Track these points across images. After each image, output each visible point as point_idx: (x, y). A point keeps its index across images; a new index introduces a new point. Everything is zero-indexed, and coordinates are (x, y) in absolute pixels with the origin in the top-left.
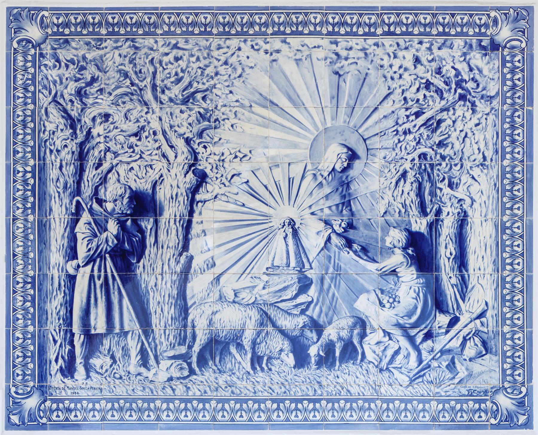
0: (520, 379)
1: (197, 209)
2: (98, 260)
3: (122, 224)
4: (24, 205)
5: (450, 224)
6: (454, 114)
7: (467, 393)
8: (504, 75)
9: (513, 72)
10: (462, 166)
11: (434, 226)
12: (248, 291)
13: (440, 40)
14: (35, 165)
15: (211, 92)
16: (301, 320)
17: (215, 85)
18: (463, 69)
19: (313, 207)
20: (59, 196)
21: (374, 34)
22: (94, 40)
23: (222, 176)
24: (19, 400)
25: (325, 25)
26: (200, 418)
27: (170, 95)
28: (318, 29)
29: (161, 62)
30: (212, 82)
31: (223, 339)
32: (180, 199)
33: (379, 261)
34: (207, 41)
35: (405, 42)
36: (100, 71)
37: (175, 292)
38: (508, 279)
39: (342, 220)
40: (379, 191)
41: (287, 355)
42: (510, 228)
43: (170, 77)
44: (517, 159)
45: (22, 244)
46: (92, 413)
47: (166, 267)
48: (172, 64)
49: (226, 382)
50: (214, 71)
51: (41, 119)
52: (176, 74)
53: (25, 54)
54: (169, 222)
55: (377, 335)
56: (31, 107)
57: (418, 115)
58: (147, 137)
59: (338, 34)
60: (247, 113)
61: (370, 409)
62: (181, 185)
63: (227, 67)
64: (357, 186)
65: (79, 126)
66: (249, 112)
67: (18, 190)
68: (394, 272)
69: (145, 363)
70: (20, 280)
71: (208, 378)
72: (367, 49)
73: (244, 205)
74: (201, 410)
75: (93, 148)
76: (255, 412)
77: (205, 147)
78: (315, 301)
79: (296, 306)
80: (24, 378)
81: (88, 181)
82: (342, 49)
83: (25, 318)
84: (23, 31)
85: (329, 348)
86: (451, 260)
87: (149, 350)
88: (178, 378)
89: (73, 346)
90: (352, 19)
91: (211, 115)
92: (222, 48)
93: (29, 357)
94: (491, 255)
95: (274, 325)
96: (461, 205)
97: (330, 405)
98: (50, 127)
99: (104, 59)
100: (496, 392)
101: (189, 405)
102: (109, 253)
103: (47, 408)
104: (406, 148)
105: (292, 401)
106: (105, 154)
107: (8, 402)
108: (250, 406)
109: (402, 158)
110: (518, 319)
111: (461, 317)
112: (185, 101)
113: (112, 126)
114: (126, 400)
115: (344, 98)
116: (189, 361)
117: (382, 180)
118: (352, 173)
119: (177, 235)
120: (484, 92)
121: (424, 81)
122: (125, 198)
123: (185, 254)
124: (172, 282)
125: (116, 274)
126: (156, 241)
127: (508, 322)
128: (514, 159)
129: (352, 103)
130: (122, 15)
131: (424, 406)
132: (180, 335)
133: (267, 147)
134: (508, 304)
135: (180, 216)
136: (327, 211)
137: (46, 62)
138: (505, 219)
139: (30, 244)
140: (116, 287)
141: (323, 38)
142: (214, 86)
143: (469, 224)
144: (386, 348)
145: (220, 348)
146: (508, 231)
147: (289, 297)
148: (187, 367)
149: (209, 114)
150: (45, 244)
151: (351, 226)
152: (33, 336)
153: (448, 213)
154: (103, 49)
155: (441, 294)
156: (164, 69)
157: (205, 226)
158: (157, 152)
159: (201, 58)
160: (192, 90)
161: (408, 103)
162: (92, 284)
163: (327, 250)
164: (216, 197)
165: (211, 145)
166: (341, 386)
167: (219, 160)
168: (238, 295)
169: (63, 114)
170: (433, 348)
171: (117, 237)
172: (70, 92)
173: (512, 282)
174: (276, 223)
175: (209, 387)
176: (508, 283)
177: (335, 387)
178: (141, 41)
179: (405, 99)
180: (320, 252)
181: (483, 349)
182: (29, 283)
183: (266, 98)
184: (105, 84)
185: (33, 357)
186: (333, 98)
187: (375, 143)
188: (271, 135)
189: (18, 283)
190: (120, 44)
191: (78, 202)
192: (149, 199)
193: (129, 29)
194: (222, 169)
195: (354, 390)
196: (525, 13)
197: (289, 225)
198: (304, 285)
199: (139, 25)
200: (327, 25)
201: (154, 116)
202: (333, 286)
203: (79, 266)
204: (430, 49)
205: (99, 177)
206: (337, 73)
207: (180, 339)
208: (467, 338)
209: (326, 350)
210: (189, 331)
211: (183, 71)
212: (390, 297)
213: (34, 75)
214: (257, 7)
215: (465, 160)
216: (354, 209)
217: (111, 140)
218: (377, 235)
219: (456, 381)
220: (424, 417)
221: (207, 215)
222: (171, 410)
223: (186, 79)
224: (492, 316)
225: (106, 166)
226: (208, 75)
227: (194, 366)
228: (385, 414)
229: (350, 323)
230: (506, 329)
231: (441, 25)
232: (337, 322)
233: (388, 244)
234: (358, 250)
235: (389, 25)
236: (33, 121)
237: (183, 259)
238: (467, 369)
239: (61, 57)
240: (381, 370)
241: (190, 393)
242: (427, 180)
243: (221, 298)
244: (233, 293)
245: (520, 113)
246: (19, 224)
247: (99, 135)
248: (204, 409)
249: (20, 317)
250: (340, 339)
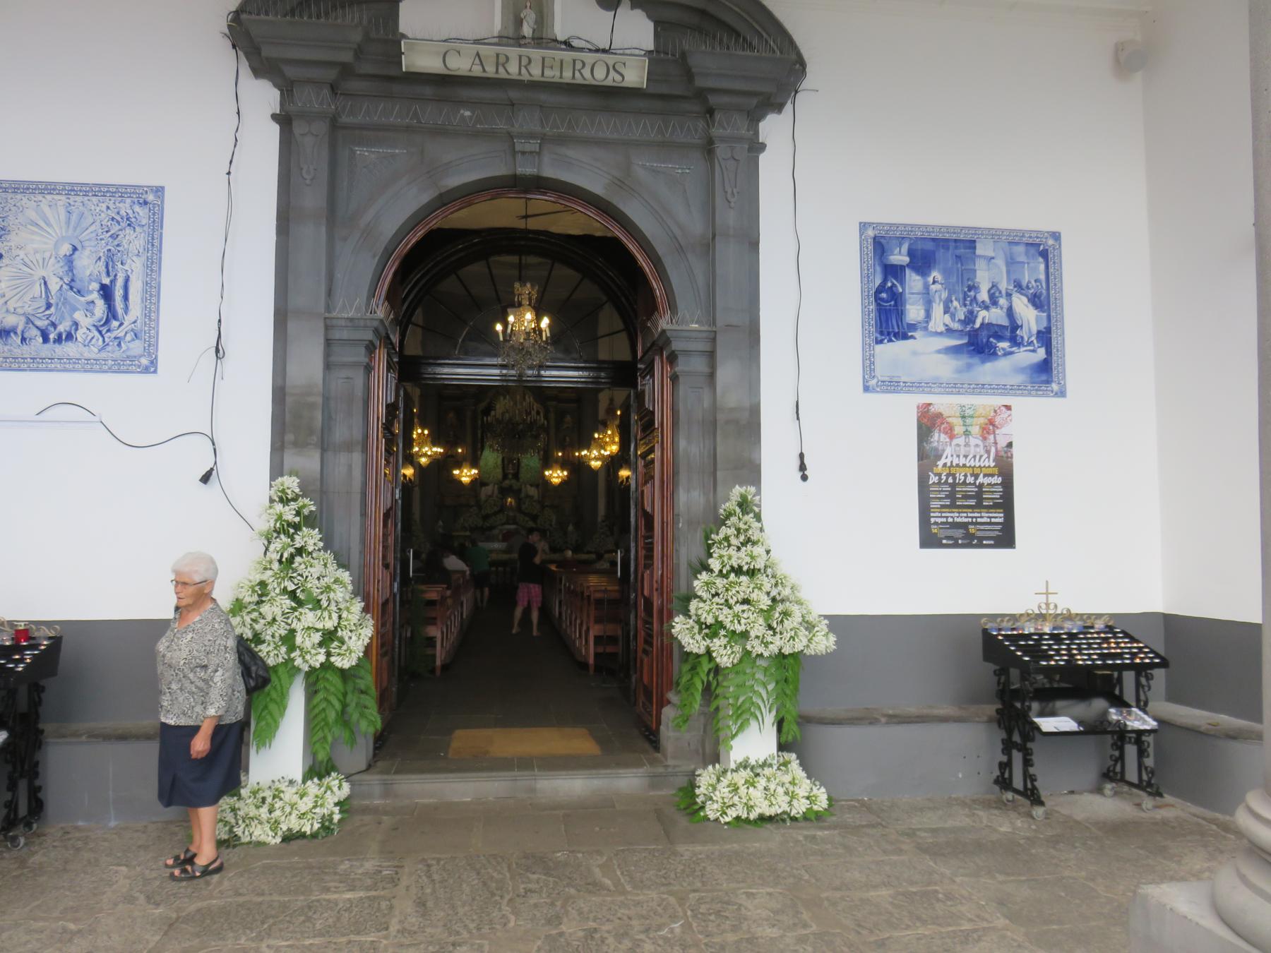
16: (46, 322)
40: (88, 265)
85: (60, 335)
100: (141, 356)
151: (73, 280)
174: (36, 278)
198: (49, 306)
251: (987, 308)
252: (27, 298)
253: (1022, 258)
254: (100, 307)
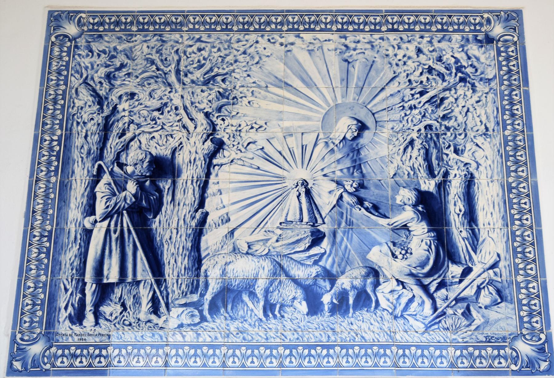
0: (538, 326)
1: (214, 172)
2: (116, 216)
3: (140, 185)
4: (47, 168)
5: (458, 185)
6: (456, 93)
7: (484, 339)
8: (500, 63)
9: (508, 59)
10: (466, 135)
11: (442, 186)
12: (261, 243)
13: (440, 35)
14: (62, 135)
15: (230, 75)
16: (314, 271)
17: (234, 70)
18: (462, 57)
19: (325, 170)
20: (82, 161)
21: (379, 31)
22: (125, 35)
23: (239, 143)
24: (24, 347)
25: (335, 24)
26: (210, 364)
27: (192, 78)
28: (329, 26)
29: (185, 53)
30: (232, 68)
31: (236, 288)
32: (198, 163)
33: (390, 217)
34: (228, 36)
35: (408, 37)
36: (129, 59)
37: (189, 245)
38: (518, 233)
39: (354, 181)
40: (389, 156)
41: (300, 303)
42: (516, 188)
43: (193, 64)
44: (517, 130)
45: (42, 202)
46: (98, 359)
47: (181, 222)
48: (195, 53)
49: (238, 328)
50: (234, 59)
51: (71, 97)
52: (199, 61)
53: (61, 46)
54: (186, 183)
55: (391, 284)
56: (63, 87)
57: (422, 93)
58: (169, 112)
59: (347, 30)
60: (263, 92)
61: (385, 355)
62: (199, 151)
63: (246, 56)
64: (367, 152)
65: (106, 103)
66: (265, 91)
67: (44, 156)
68: (405, 227)
69: (155, 310)
70: (37, 234)
71: (220, 325)
72: (374, 42)
73: (259, 168)
74: (211, 356)
75: (118, 121)
76: (267, 358)
77: (223, 120)
78: (328, 252)
79: (309, 257)
80: (31, 324)
81: (111, 148)
82: (350, 42)
83: (38, 268)
84: (62, 29)
85: (343, 296)
86: (460, 216)
87: (160, 298)
88: (189, 325)
89: (84, 295)
90: (359, 19)
91: (230, 94)
92: (241, 41)
93: (38, 305)
94: (500, 211)
95: (287, 275)
96: (467, 168)
97: (344, 351)
98: (78, 103)
99: (133, 50)
100: (515, 338)
101: (199, 351)
102: (126, 210)
103: (52, 354)
104: (412, 121)
105: (305, 347)
106: (129, 125)
107: (12, 348)
108: (262, 352)
109: (409, 129)
110: (531, 269)
111: (474, 268)
112: (206, 83)
113: (137, 103)
114: (134, 347)
115: (353, 80)
116: (200, 308)
117: (391, 147)
118: (361, 141)
119: (194, 194)
120: (483, 76)
121: (427, 67)
122: (145, 163)
123: (200, 210)
124: (186, 236)
125: (132, 229)
126: (173, 199)
127: (521, 272)
128: (514, 130)
129: (361, 84)
130: (152, 16)
131: (441, 352)
132: (192, 284)
133: (281, 120)
134: (519, 255)
135: (197, 177)
136: (338, 173)
137: (80, 53)
138: (511, 180)
139: (50, 202)
140: (131, 240)
141: (333, 34)
142: (233, 71)
143: (476, 185)
144: (399, 296)
145: (232, 296)
146: (514, 191)
147: (302, 249)
148: (198, 314)
149: (227, 93)
150: (64, 202)
151: (361, 186)
152: (45, 284)
153: (455, 175)
154: (133, 42)
155: (452, 246)
156: (188, 57)
157: (221, 186)
158: (178, 124)
159: (222, 49)
160: (213, 74)
161: (412, 84)
162: (108, 238)
163: (339, 207)
164: (232, 161)
165: (229, 118)
166: (355, 333)
167: (236, 131)
168: (251, 247)
169: (92, 93)
170: (447, 297)
171: (135, 196)
172: (99, 76)
173: (522, 236)
174: (290, 183)
175: (221, 334)
176: (518, 236)
177: (349, 333)
178: (168, 36)
179: (410, 81)
180: (332, 209)
181: (498, 297)
182: (46, 236)
183: (281, 80)
184: (133, 69)
185: (42, 304)
186: (343, 80)
187: (383, 116)
188: (285, 110)
189: (35, 236)
190: (148, 38)
191: (100, 166)
192: (168, 163)
193: (157, 27)
194: (239, 138)
195: (369, 336)
196: (514, 15)
197: (302, 185)
198: (317, 238)
199: (166, 23)
200: (337, 24)
201: (177, 95)
202: (345, 239)
203: (96, 221)
204: (430, 42)
205: (122, 145)
206: (346, 61)
207: (192, 287)
208: (482, 287)
209: (340, 298)
210: (202, 279)
211: (205, 59)
212: (402, 249)
213: (68, 63)
214: (273, 10)
215: (469, 130)
216: (364, 171)
217: (135, 114)
218: (388, 194)
219: (473, 327)
220: (442, 363)
221: (224, 177)
222: (180, 356)
223: (208, 65)
224: (505, 267)
225: (129, 135)
226: (228, 62)
227: (206, 313)
228: (402, 360)
229: (363, 273)
230: (520, 279)
231: (440, 23)
232: (350, 272)
233: (398, 202)
234: (369, 207)
235: (393, 24)
236: (64, 98)
237: (198, 215)
238: (483, 316)
239: (94, 48)
240: (396, 317)
241: (201, 340)
242: (433, 148)
243: (234, 249)
244: (247, 245)
245: (517, 92)
246: (42, 185)
247: (124, 110)
248: (214, 355)
249: (33, 267)
250: (353, 287)
252: (274, 222)
254: (420, 236)
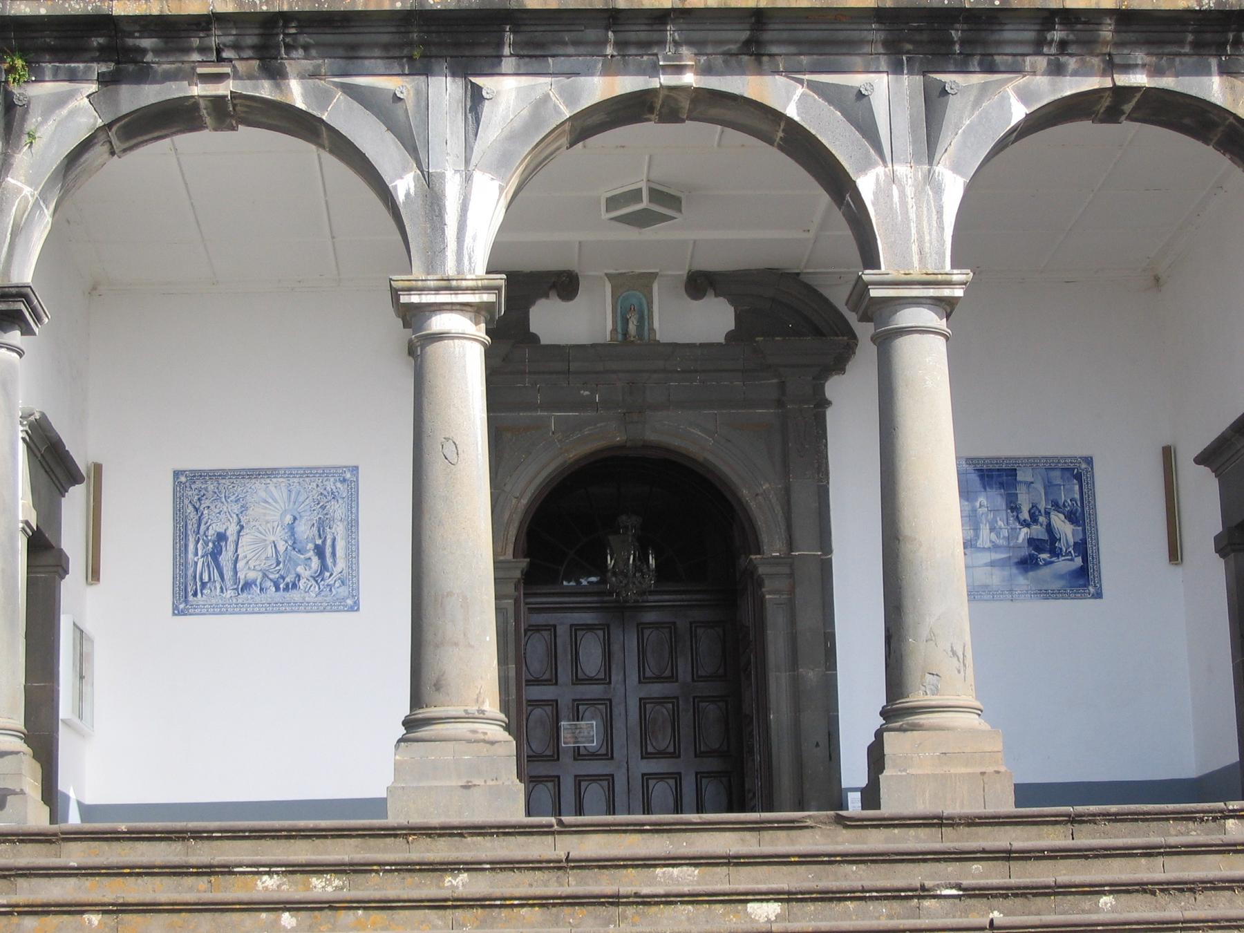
40: (305, 530)
85: (287, 585)
198: (278, 563)
221: (244, 540)
251: (1028, 526)
253: (1059, 481)
